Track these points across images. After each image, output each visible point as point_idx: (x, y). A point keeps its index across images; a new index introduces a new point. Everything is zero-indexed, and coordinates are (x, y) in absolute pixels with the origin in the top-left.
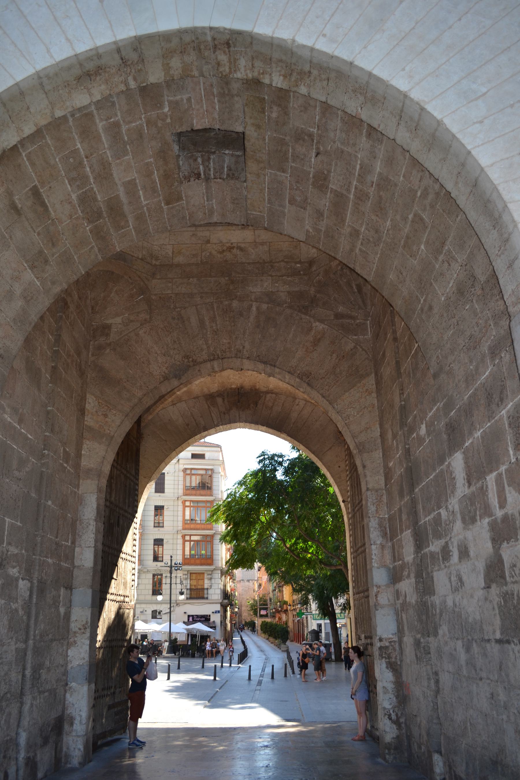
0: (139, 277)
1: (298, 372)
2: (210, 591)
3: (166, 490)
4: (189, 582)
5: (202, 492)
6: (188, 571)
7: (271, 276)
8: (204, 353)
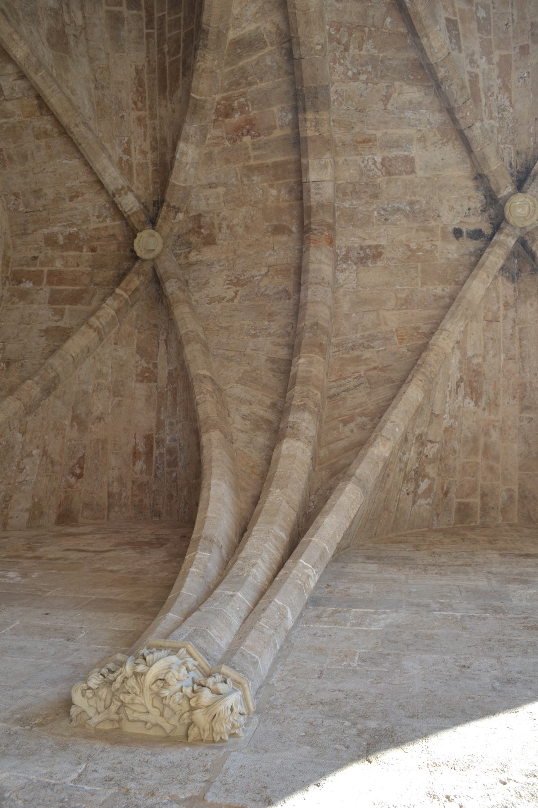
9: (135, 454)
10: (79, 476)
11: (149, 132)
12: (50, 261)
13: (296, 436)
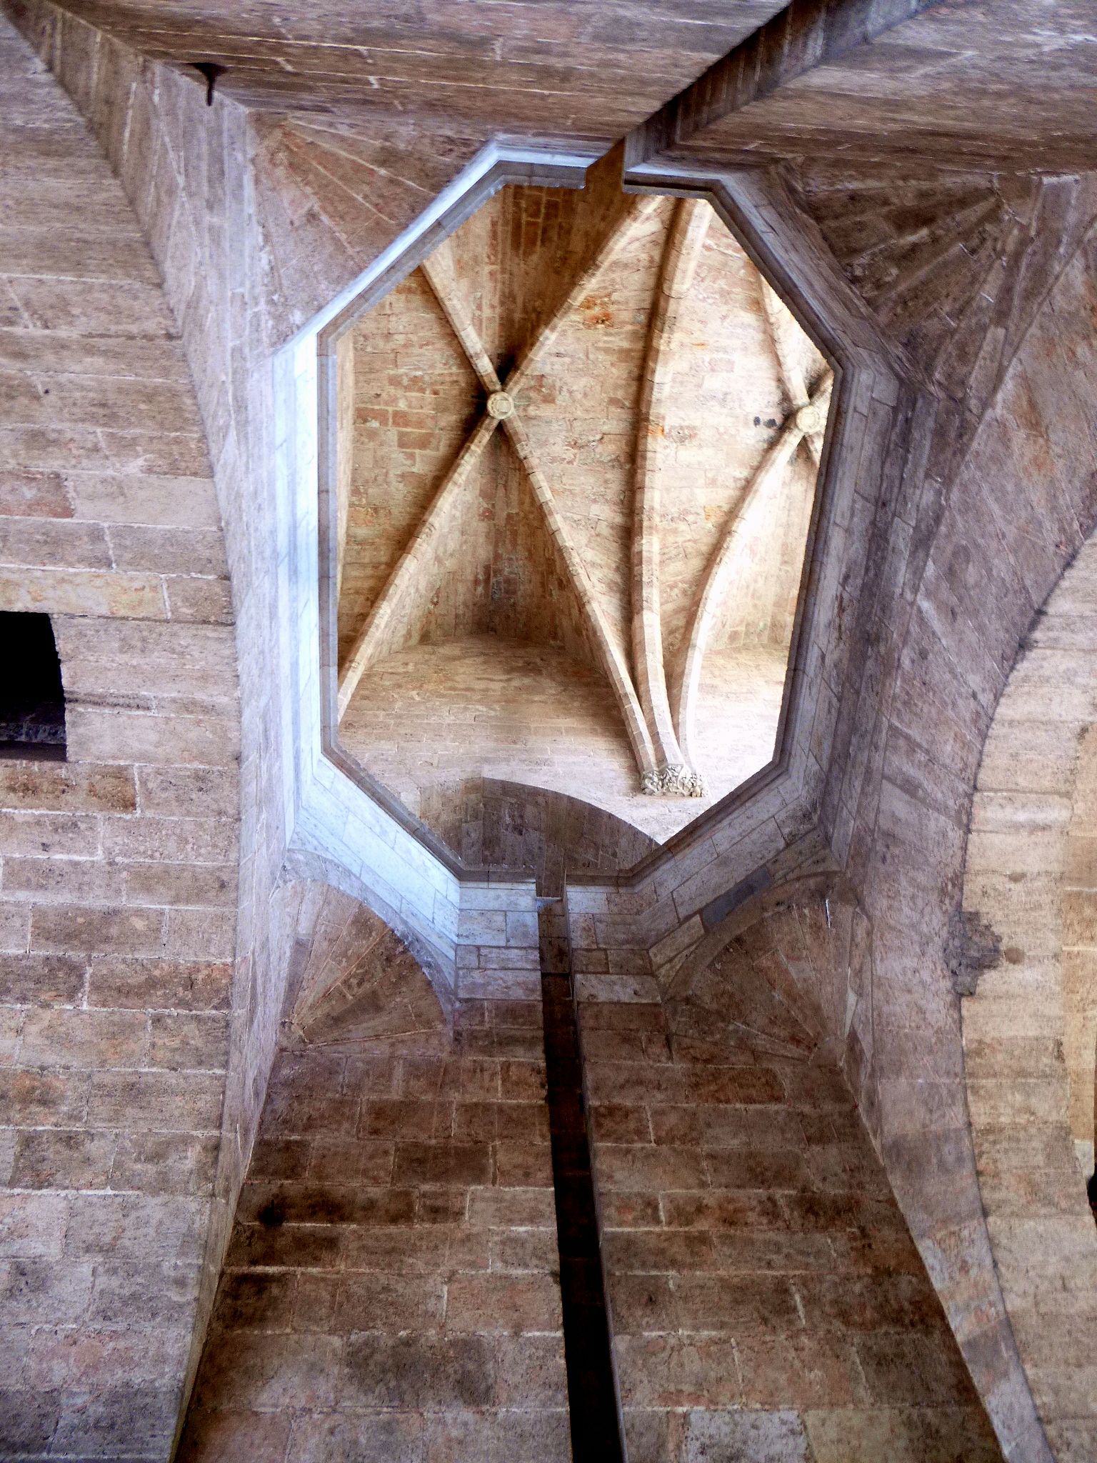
0: (798, 879)
1: (1076, 526)
7: (894, 515)
8: (950, 834)
9: (476, 582)
10: (436, 604)
11: (499, 286)
12: (394, 400)
13: (650, 609)
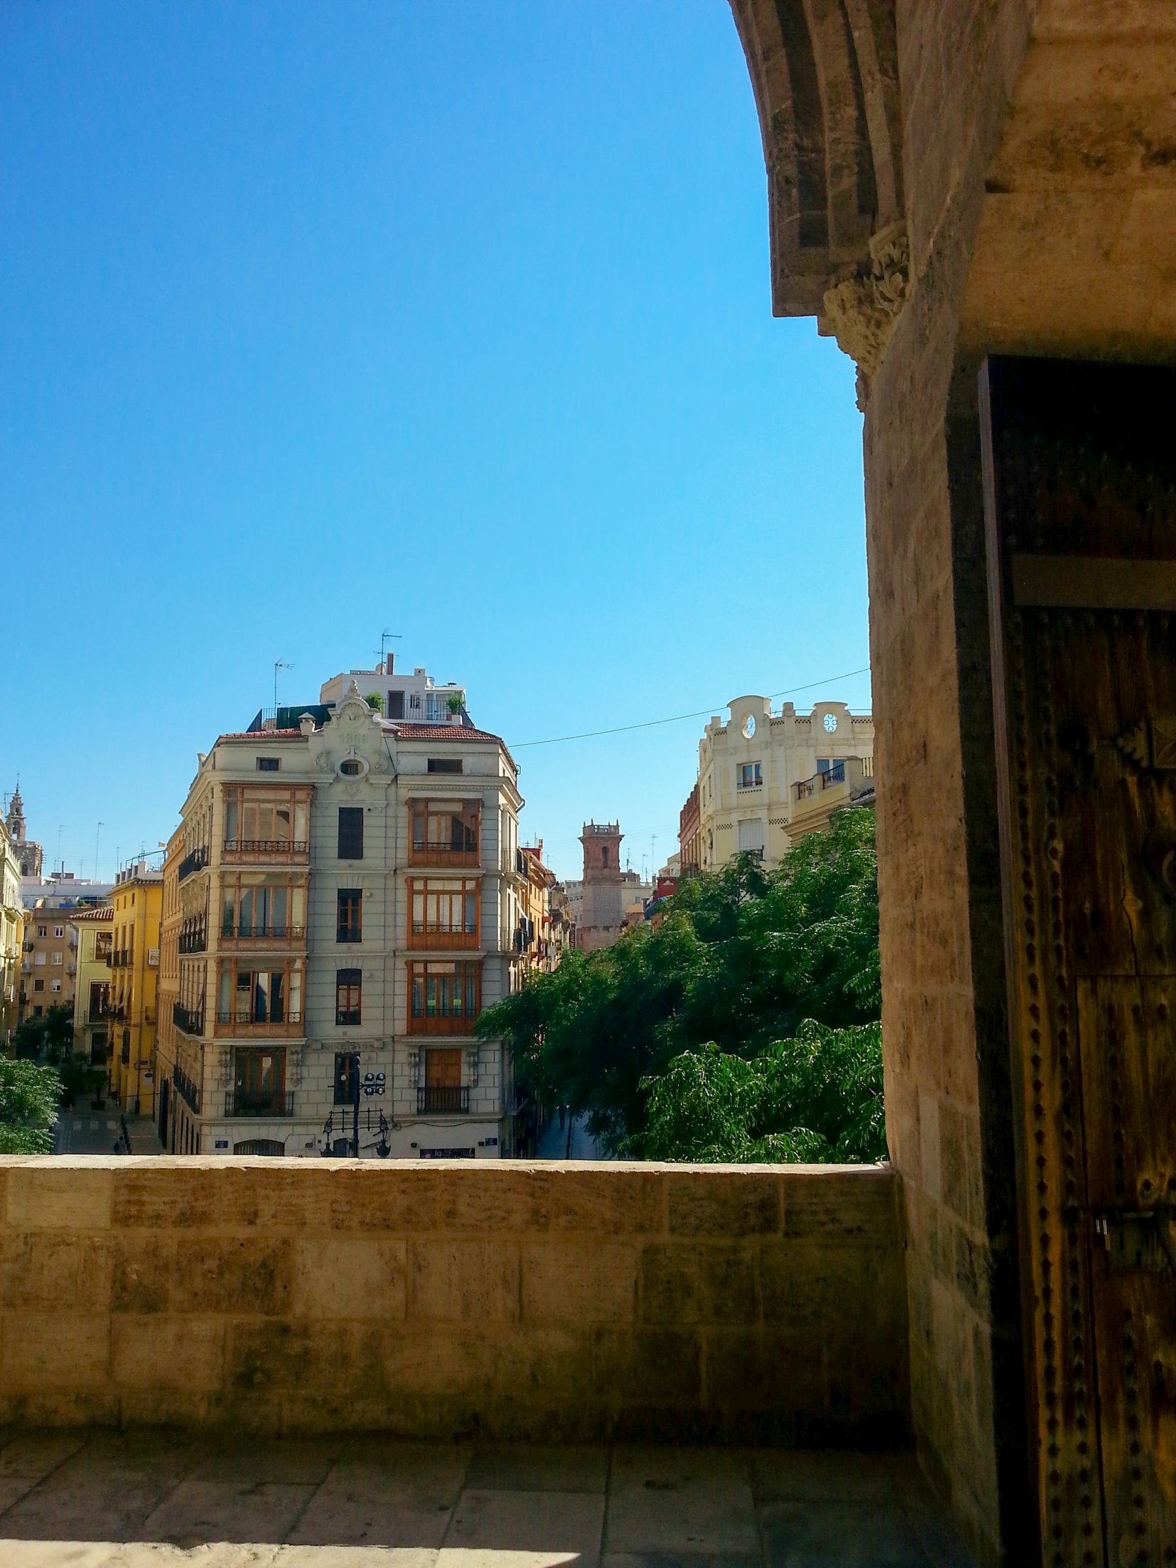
2: (475, 1094)
3: (366, 852)
4: (423, 1072)
5: (455, 857)
6: (420, 1047)
